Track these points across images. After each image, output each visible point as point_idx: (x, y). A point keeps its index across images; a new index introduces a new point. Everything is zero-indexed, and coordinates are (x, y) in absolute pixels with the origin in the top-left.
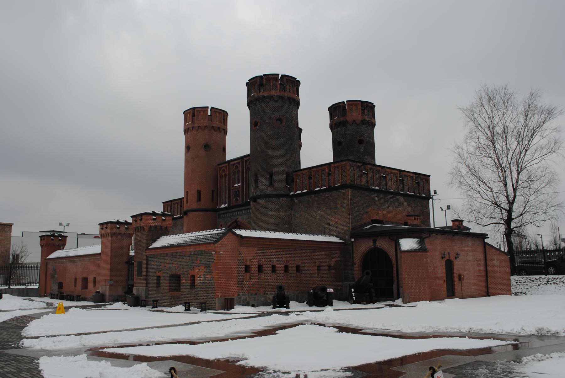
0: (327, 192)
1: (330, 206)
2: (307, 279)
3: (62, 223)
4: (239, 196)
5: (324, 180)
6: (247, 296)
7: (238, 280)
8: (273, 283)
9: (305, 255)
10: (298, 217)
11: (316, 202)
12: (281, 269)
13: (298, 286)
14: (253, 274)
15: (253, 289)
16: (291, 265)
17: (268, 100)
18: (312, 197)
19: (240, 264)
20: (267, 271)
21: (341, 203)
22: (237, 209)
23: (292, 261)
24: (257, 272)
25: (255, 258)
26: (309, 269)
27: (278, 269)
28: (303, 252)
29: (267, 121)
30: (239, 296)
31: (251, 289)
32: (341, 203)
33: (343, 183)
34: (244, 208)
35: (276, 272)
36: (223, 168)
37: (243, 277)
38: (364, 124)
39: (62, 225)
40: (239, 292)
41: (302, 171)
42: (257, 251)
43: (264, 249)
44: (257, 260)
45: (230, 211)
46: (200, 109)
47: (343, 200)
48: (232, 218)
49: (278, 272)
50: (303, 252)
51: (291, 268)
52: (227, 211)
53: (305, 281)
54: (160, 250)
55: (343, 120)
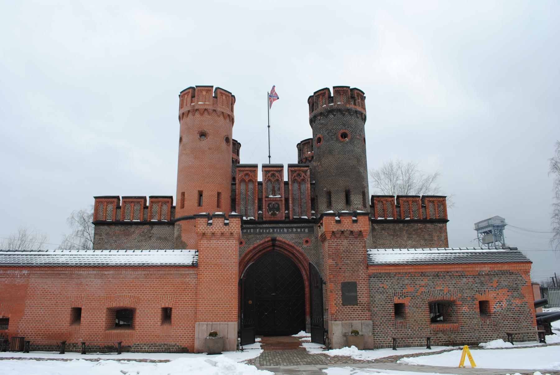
0: (420, 223)
1: (424, 237)
4: (278, 209)
5: (415, 211)
10: (380, 245)
11: (405, 231)
17: (358, 115)
18: (400, 226)
21: (438, 236)
22: (274, 225)
29: (358, 137)
32: (438, 236)
33: (439, 218)
34: (288, 225)
36: (246, 172)
41: (386, 198)
45: (261, 226)
46: (223, 92)
47: (440, 233)
48: (264, 235)
52: (253, 225)
54: (410, 267)
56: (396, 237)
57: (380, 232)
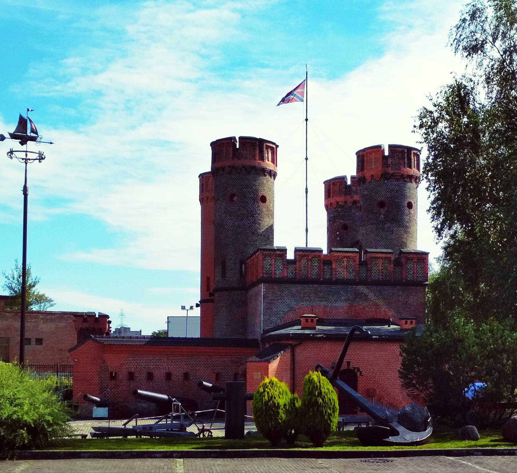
3: (184, 307)
35: (153, 380)
38: (386, 179)
39: (185, 308)
44: (126, 367)
55: (361, 176)
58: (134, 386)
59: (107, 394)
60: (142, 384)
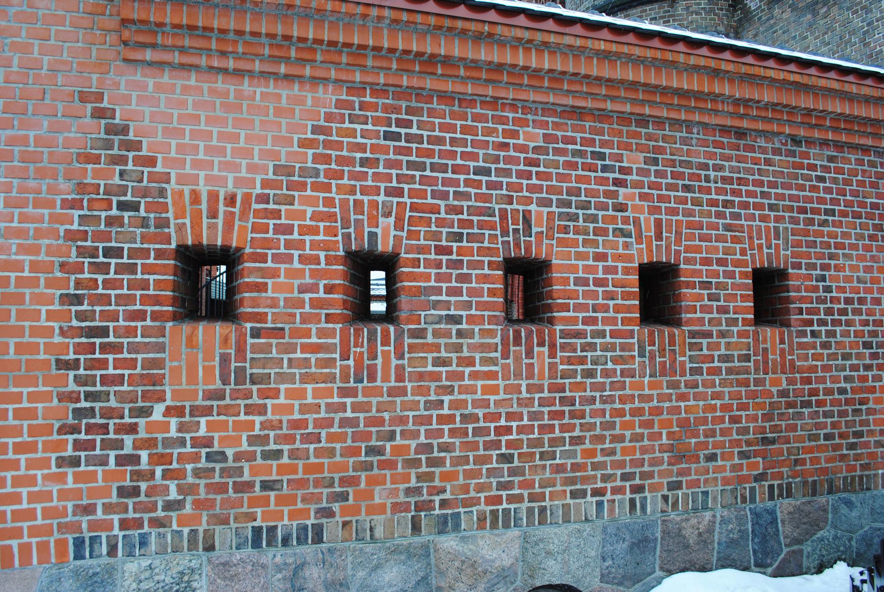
2: (847, 379)
6: (184, 561)
7: (73, 397)
8: (510, 416)
9: (828, 190)
12: (610, 296)
13: (766, 441)
14: (278, 332)
15: (266, 486)
16: (706, 262)
19: (104, 236)
20: (447, 305)
23: (711, 226)
24: (492, 320)
25: (302, 186)
26: (861, 301)
27: (573, 295)
28: (812, 167)
30: (87, 562)
31: (244, 487)
35: (551, 321)
37: (150, 364)
40: (84, 521)
42: (329, 117)
43: (410, 111)
44: (329, 202)
49: (574, 321)
50: (812, 167)
51: (706, 285)
53: (829, 392)
56: (825, 9)
57: (768, 20)
58: (400, 378)
59: (144, 455)
60: (470, 362)
